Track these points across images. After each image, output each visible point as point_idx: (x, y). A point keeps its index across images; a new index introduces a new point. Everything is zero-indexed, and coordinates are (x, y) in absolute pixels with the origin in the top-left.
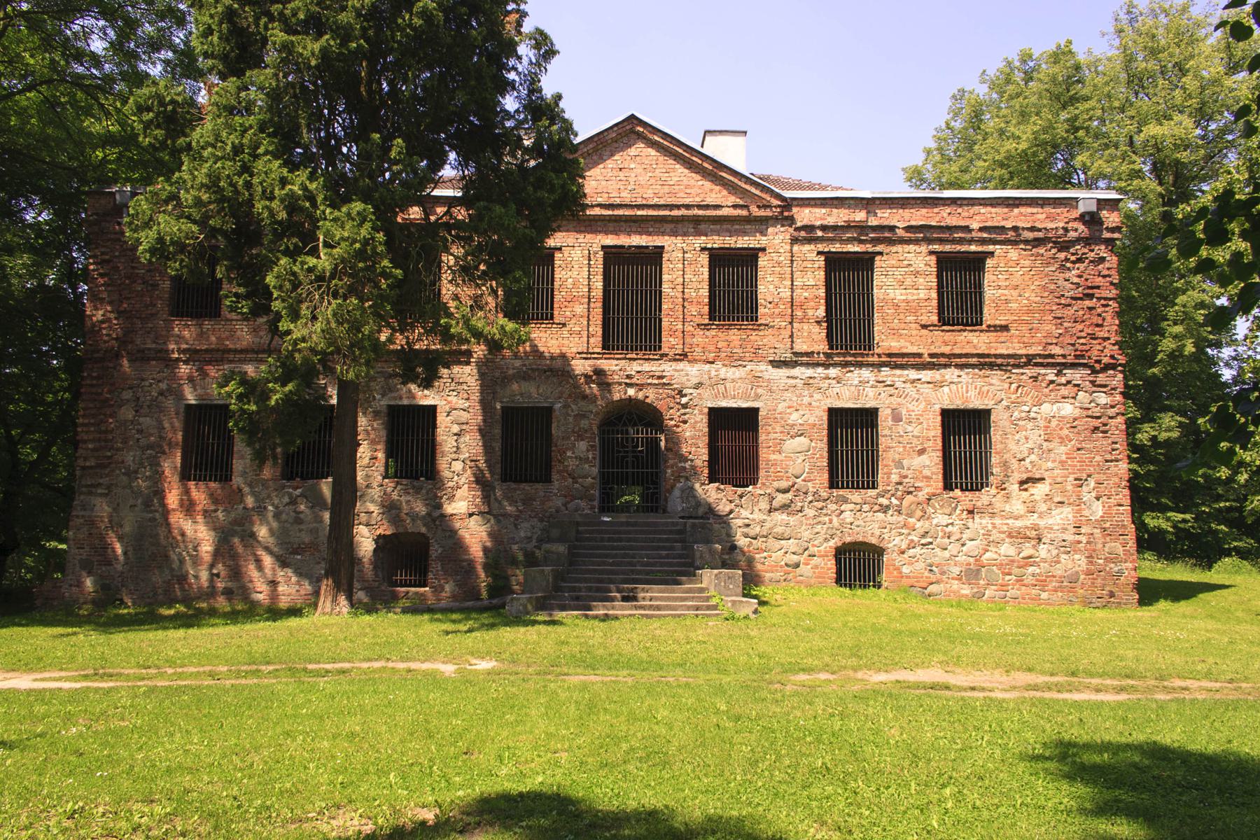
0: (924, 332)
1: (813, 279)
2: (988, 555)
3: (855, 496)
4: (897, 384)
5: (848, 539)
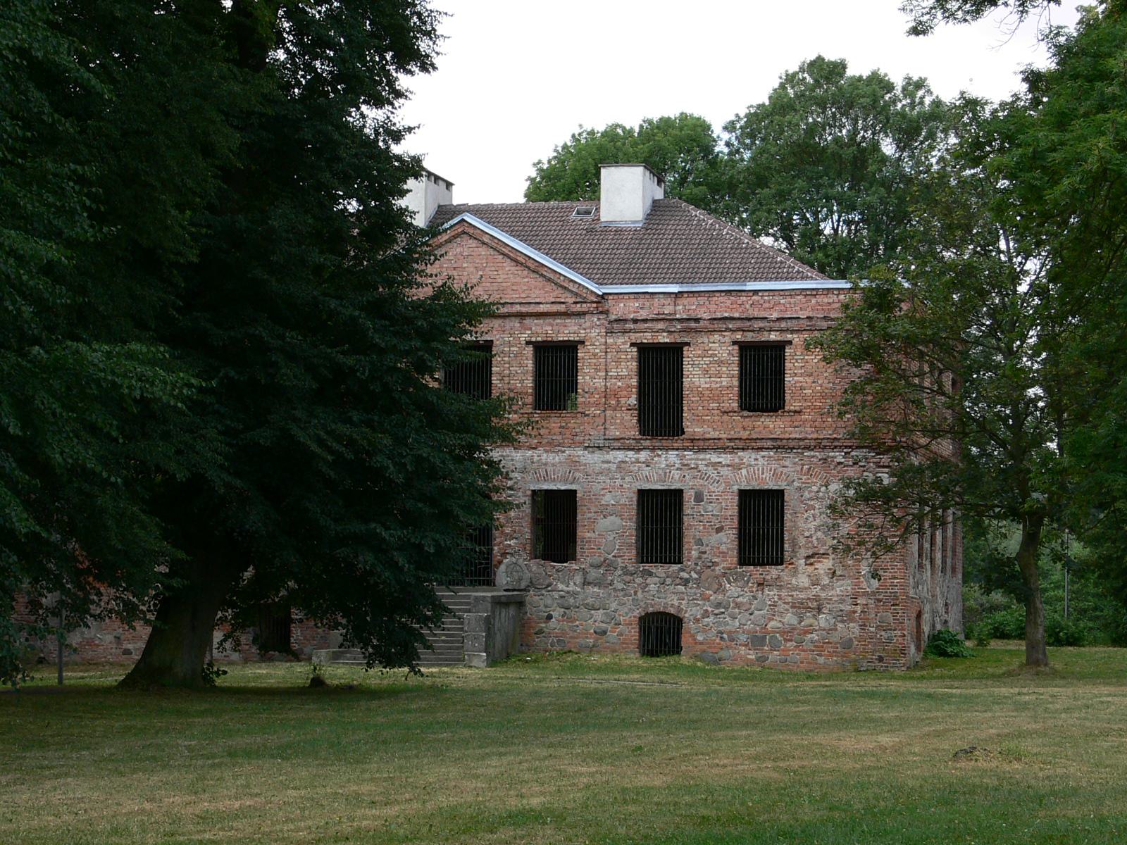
0: (725, 417)
1: (625, 372)
2: (772, 623)
3: (660, 570)
4: (701, 467)
5: (651, 610)
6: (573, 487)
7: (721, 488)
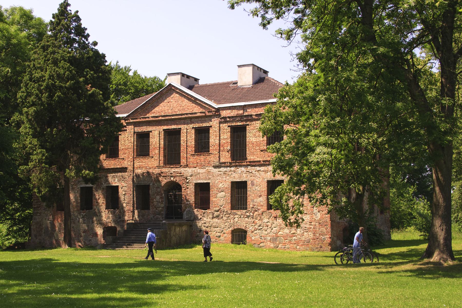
0: (262, 153)
1: (226, 136)
2: (280, 233)
3: (239, 212)
4: (253, 172)
5: (236, 228)
6: (209, 181)
7: (261, 180)
